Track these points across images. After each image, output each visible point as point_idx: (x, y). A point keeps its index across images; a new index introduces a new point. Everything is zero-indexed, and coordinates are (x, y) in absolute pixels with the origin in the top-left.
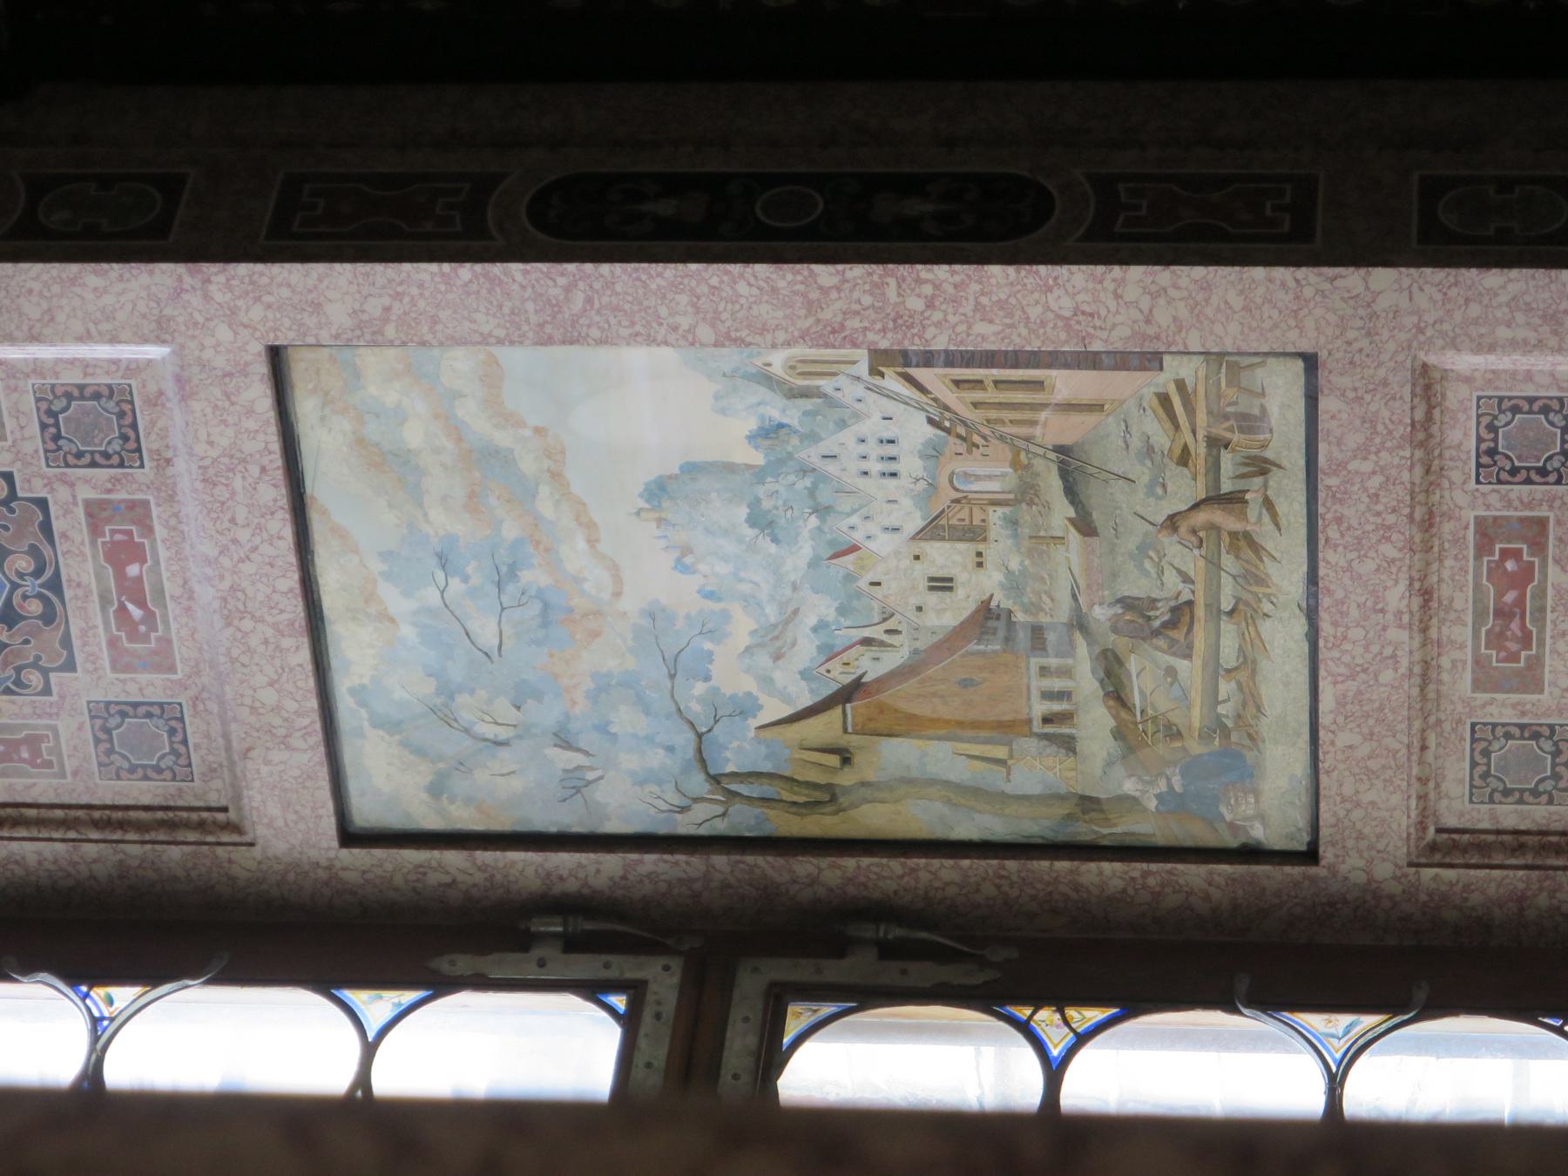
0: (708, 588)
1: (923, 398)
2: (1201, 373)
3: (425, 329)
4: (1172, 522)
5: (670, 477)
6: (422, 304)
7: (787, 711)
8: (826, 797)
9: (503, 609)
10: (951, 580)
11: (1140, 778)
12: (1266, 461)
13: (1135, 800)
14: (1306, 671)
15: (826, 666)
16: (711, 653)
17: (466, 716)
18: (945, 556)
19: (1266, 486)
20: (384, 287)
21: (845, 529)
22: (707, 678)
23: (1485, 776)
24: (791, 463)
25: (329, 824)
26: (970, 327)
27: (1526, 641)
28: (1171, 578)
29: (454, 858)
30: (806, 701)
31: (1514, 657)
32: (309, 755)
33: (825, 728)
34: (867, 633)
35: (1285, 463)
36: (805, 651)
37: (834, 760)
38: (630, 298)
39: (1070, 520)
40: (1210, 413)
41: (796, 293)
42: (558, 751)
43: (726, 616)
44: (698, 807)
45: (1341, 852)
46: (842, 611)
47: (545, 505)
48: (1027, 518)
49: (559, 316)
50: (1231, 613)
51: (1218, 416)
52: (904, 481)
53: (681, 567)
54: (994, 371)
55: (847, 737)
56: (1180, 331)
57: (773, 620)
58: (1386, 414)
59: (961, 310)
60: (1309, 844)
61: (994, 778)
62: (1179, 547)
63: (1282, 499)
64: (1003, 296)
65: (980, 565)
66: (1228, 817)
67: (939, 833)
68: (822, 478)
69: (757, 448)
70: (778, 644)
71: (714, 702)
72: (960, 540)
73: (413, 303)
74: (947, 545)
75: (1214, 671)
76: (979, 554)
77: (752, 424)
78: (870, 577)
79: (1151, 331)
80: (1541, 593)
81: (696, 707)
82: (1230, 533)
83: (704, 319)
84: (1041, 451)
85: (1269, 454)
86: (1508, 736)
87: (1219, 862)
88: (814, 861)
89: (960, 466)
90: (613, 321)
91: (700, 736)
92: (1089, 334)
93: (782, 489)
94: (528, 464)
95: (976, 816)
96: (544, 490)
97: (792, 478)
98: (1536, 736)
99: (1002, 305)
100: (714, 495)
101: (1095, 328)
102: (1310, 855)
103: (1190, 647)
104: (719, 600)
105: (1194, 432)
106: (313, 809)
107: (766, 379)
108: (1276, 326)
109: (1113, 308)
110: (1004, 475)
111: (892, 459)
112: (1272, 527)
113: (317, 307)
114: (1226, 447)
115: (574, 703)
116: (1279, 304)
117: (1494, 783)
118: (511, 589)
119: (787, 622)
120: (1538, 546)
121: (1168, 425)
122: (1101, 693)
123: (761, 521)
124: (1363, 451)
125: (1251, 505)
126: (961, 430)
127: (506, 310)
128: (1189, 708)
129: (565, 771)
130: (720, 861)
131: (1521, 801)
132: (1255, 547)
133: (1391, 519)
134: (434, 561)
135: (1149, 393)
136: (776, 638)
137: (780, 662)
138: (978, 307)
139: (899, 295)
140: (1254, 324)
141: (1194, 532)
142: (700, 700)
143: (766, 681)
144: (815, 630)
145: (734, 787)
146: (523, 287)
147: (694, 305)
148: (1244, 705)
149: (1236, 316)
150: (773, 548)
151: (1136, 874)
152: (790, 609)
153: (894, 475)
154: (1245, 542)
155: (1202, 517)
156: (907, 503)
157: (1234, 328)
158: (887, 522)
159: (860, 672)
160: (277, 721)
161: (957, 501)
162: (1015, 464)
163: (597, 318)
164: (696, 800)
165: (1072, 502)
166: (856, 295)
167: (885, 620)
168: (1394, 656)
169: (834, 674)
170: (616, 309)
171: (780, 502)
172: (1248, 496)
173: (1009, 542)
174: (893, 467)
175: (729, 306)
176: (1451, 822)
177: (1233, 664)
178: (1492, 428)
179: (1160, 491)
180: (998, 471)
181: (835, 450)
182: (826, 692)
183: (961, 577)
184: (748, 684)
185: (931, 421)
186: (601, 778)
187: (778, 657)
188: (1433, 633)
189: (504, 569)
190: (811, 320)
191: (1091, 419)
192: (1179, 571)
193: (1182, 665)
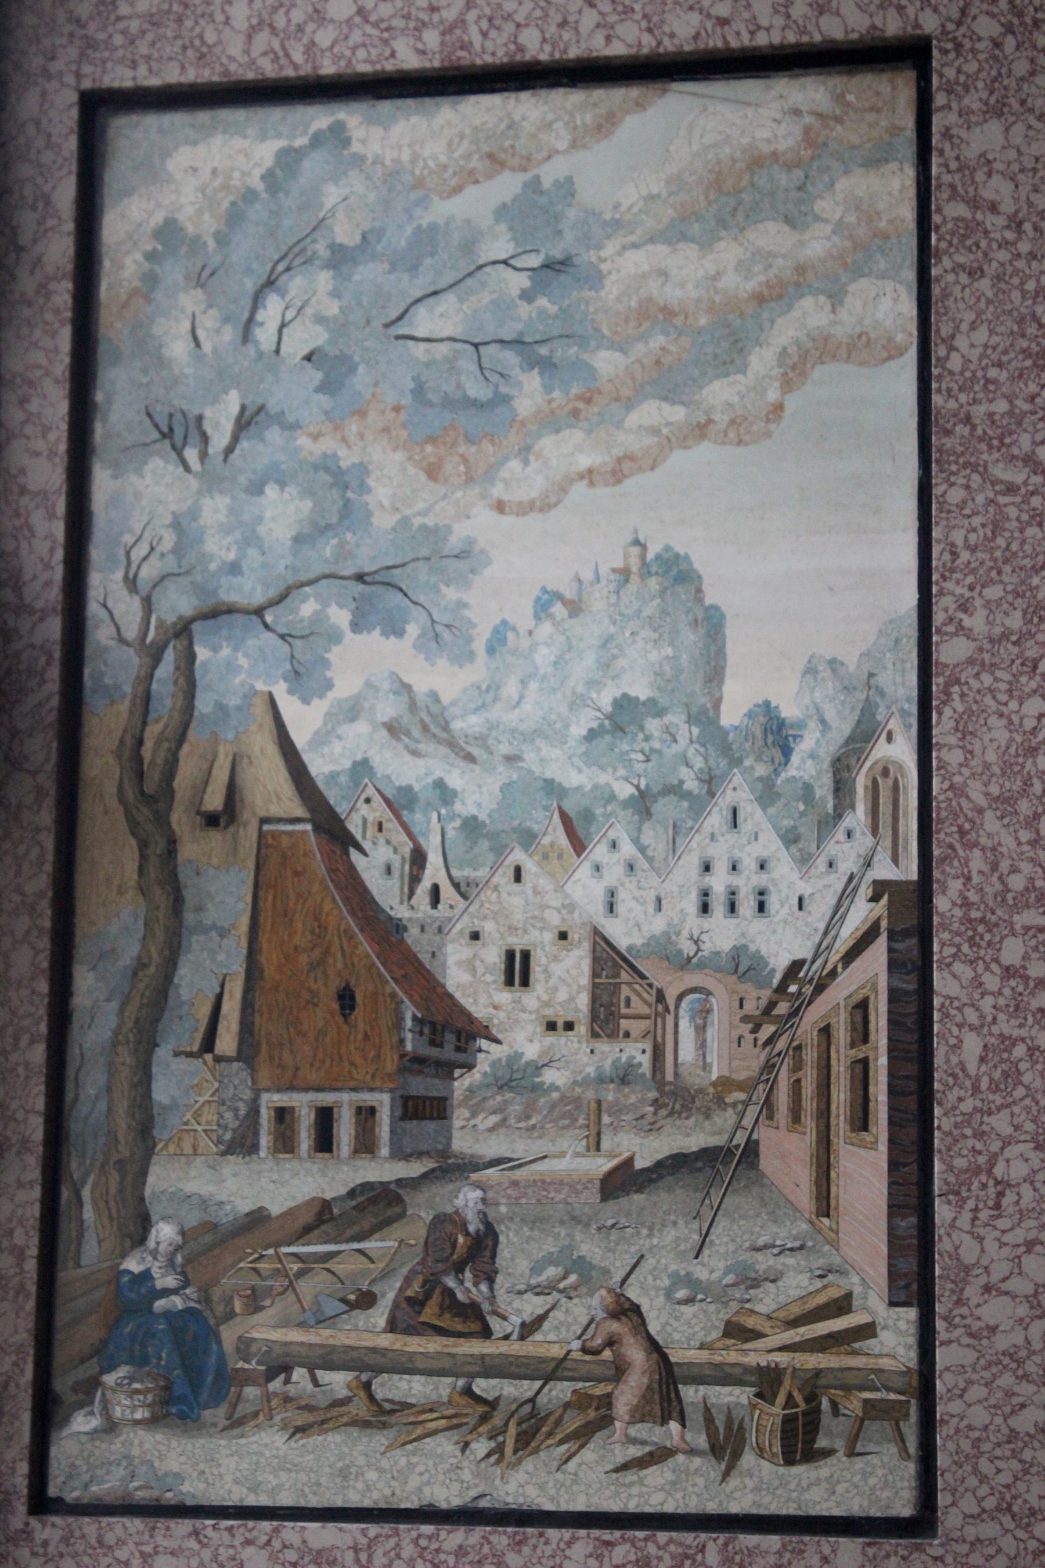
0: (510, 635)
1: (835, 957)
2: (886, 1363)
3: (960, 259)
4: (627, 1311)
5: (699, 590)
6: (1003, 255)
7: (300, 738)
8: (150, 787)
9: (476, 346)
10: (525, 982)
11: (178, 1248)
12: (736, 1455)
13: (142, 1240)
14: (367, 1503)
15: (377, 798)
16: (400, 633)
17: (296, 284)
18: (565, 979)
19: (692, 1452)
20: (1030, 204)
21: (612, 834)
22: (356, 627)
24: (723, 763)
26: (972, 1028)
28: (532, 1306)
29: (59, 249)
30: (317, 766)
32: (241, 56)
33: (270, 791)
34: (434, 859)
35: (733, 1482)
36: (402, 769)
37: (214, 801)
38: (1014, 547)
39: (629, 1161)
40: (818, 1373)
41: (1027, 783)
42: (235, 410)
43: (464, 657)
44: (136, 604)
45: (51, 1549)
46: (472, 826)
47: (652, 412)
48: (633, 1099)
49: (984, 447)
50: (468, 1392)
51: (813, 1386)
52: (693, 922)
53: (544, 604)
54: (883, 1060)
55: (254, 824)
56: (971, 1335)
57: (457, 725)
59: (1002, 1017)
60: (59, 1500)
62: (584, 1320)
63: (669, 1476)
64: (1027, 1078)
65: (551, 1026)
66: (109, 1379)
67: (84, 948)
68: (699, 806)
69: (750, 715)
70: (416, 732)
72: (594, 999)
73: (1004, 244)
74: (585, 980)
75: (367, 1365)
76: (569, 1026)
77: (789, 711)
78: (530, 866)
79: (972, 1292)
81: (308, 608)
82: (609, 1395)
83: (981, 650)
84: (748, 1122)
85: (748, 1459)
87: (37, 1364)
88: (50, 766)
89: (721, 1004)
90: (976, 521)
91: (259, 612)
92: (964, 1201)
93: (676, 749)
94: (721, 393)
95: (114, 1005)
96: (677, 414)
97: (699, 763)
99: (1013, 1075)
100: (669, 651)
101: (976, 1210)
102: (41, 1504)
103: (410, 1330)
104: (491, 650)
105: (782, 1349)
106: (148, 58)
107: (865, 733)
108: (983, 1479)
109: (1007, 1238)
110: (706, 1067)
111: (732, 908)
112: (620, 1459)
113: (997, 110)
114: (758, 1395)
115: (315, 437)
116: (1021, 1486)
118: (511, 358)
119: (452, 744)
121: (796, 1310)
122: (328, 1196)
123: (625, 716)
125: (658, 1430)
126: (782, 1008)
127: (993, 373)
128: (302, 1325)
129: (200, 419)
130: (54, 628)
132: (583, 1435)
134: (557, 254)
135: (853, 1282)
136: (425, 728)
137: (384, 733)
138: (1008, 1042)
139: (1027, 929)
140: (986, 1447)
141: (611, 1342)
142: (319, 617)
143: (352, 711)
144: (440, 784)
145: (169, 656)
146: (1032, 399)
147: (1005, 636)
148: (309, 1408)
149: (999, 1420)
150: (578, 730)
151: (19, 1238)
152: (475, 752)
153: (705, 908)
154: (597, 1417)
155: (636, 1354)
156: (657, 925)
157: (979, 1416)
158: (622, 895)
159: (367, 845)
160: (297, 16)
161: (661, 997)
162: (725, 1084)
163: (980, 499)
164: (148, 603)
165: (659, 1164)
166: (1026, 867)
167: (456, 886)
169: (364, 810)
170: (997, 527)
171: (656, 745)
172: (674, 1426)
173: (590, 1070)
174: (719, 908)
175: (1004, 687)
177: (379, 1394)
179: (681, 1294)
180: (712, 1058)
181: (746, 827)
182: (332, 796)
183: (530, 999)
184: (346, 685)
185: (797, 965)
186: (187, 468)
187: (393, 729)
189: (543, 350)
190: (982, 801)
191: (804, 1197)
192: (541, 1319)
193: (379, 1316)
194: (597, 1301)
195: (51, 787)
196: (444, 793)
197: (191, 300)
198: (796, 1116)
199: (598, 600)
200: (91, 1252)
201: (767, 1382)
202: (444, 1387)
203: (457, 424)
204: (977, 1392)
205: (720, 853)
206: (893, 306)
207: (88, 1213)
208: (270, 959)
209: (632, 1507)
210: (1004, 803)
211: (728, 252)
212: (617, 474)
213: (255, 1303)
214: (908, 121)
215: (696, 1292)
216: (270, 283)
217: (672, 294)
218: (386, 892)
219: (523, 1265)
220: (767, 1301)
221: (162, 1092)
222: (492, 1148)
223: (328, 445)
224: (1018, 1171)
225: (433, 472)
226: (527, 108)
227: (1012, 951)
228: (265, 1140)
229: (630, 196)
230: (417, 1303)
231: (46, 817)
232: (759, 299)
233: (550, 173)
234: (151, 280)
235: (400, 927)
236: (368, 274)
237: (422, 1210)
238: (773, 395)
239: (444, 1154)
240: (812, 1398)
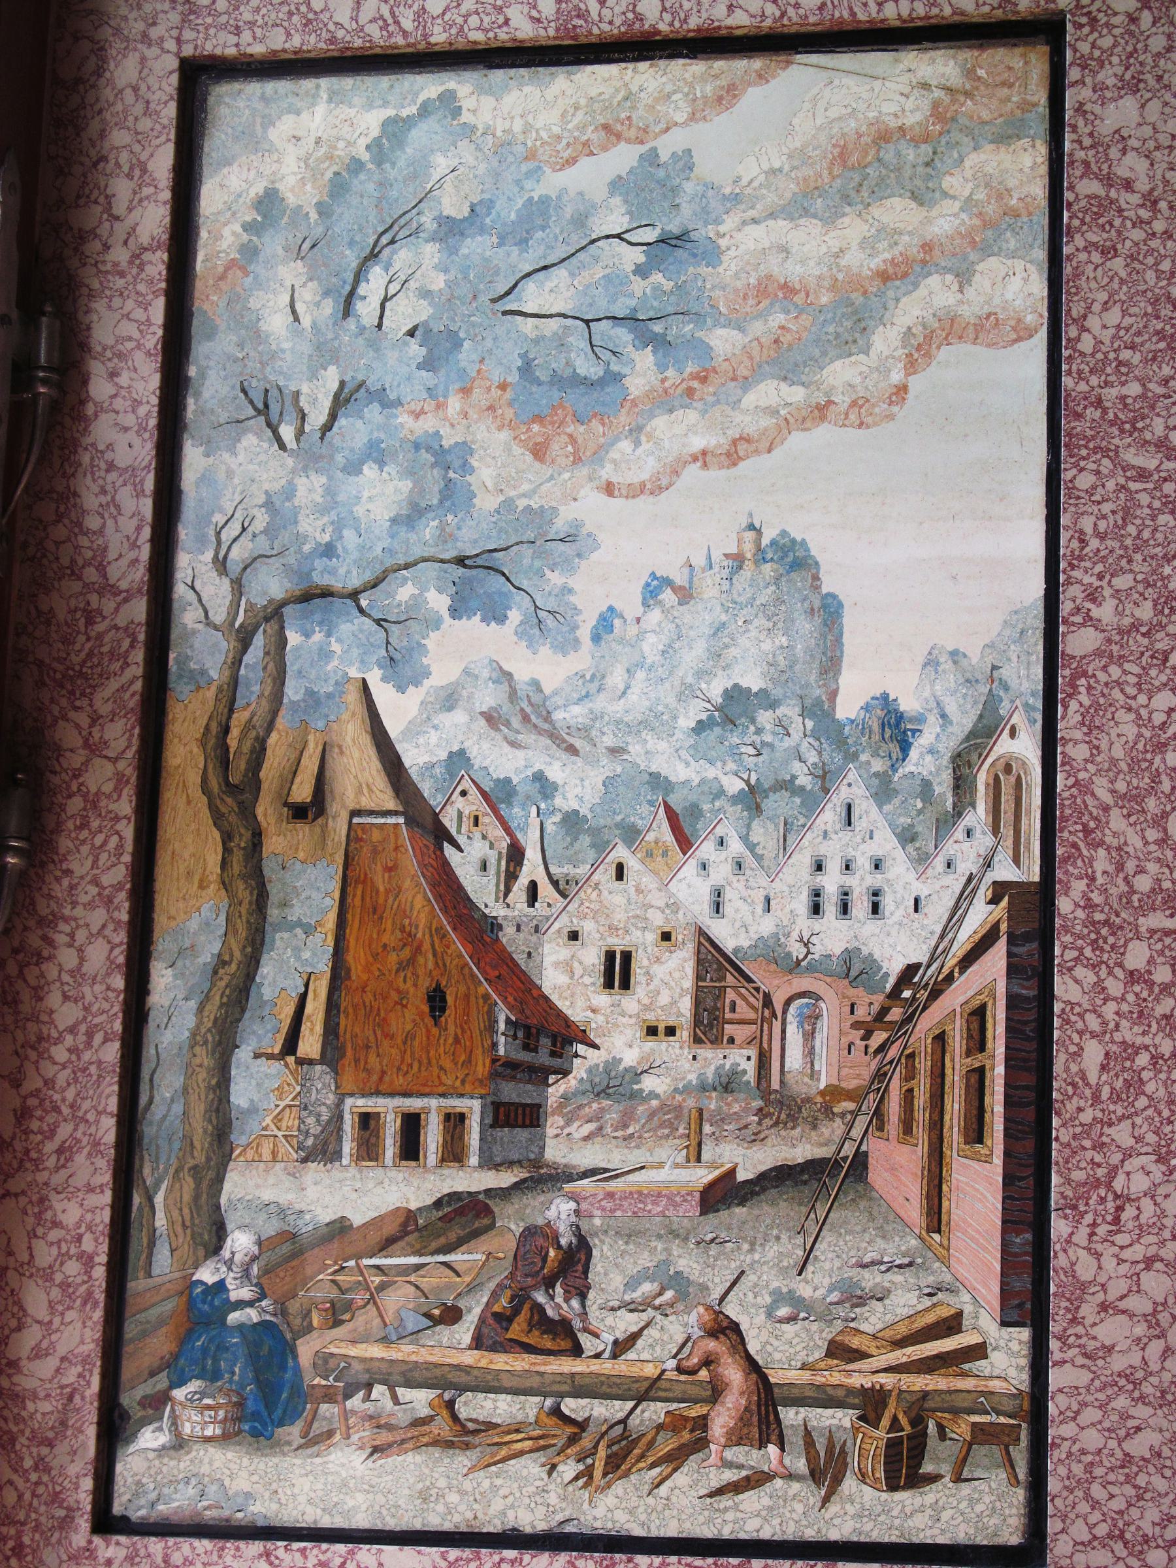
0: (617, 622)
1: (951, 962)
2: (996, 1385)
3: (1095, 238)
4: (725, 1329)
5: (816, 578)
6: (1137, 234)
8: (235, 778)
9: (587, 322)
10: (626, 985)
11: (254, 1258)
12: (837, 1480)
13: (217, 1249)
14: (447, 1526)
15: (473, 791)
16: (501, 620)
17: (402, 257)
18: (668, 982)
19: (790, 1476)
20: (1166, 182)
21: (719, 831)
22: (455, 612)
24: (838, 758)
25: (223, 45)
26: (1093, 1035)
28: (626, 1323)
29: (153, 219)
30: (413, 757)
33: (359, 781)
34: (532, 855)
35: (833, 1508)
36: (500, 760)
37: (302, 792)
38: (1146, 534)
39: (732, 1172)
40: (925, 1395)
41: (1156, 779)
42: (335, 386)
43: (570, 644)
44: (225, 585)
46: (572, 821)
47: (769, 393)
48: (736, 1108)
49: (1115, 431)
50: (556, 1412)
51: (920, 1408)
52: (804, 925)
54: (1000, 1070)
55: (344, 816)
56: (1085, 1355)
57: (558, 716)
59: (1124, 1023)
60: (125, 1519)
61: (260, 1034)
62: (680, 1339)
63: (766, 1501)
64: (1150, 1088)
65: (652, 1031)
66: (179, 1394)
67: (163, 944)
68: (812, 803)
69: (867, 708)
70: (516, 722)
71: (414, 617)
72: (697, 1003)
73: (1139, 223)
74: (688, 983)
75: (450, 1383)
76: (671, 1031)
77: (908, 704)
78: (633, 864)
79: (1087, 1311)
81: (405, 593)
82: (705, 1417)
83: (1109, 641)
84: (856, 1133)
85: (850, 1484)
87: (104, 1376)
88: (130, 754)
89: (831, 1009)
90: (1107, 508)
91: (354, 595)
92: (1082, 1215)
93: (788, 742)
94: (842, 375)
95: (193, 1004)
96: (796, 394)
97: (812, 758)
99: (1135, 1084)
100: (784, 641)
101: (1094, 1225)
102: (106, 1522)
103: (495, 1348)
104: (596, 638)
105: (886, 1370)
106: (252, 24)
107: (986, 730)
108: (1095, 1505)
109: (1126, 1254)
110: (814, 1075)
111: (845, 909)
112: (715, 1484)
113: (1133, 86)
114: (859, 1418)
115: (417, 415)
116: (1135, 1513)
118: (623, 336)
119: (553, 735)
121: (903, 1330)
122: (413, 1206)
123: (735, 709)
125: (755, 1454)
126: (896, 1014)
127: (1126, 355)
128: (385, 1340)
129: (297, 394)
130: (139, 610)
132: (676, 1459)
134: (674, 228)
135: (963, 1301)
136: (526, 718)
137: (483, 722)
138: (1131, 1050)
139: (1152, 932)
140: (1099, 1471)
141: (708, 1362)
142: (417, 602)
143: (449, 700)
144: (539, 777)
145: (259, 641)
146: (1165, 382)
147: (1135, 627)
148: (390, 1427)
149: (1113, 1444)
150: (687, 722)
151: (88, 1244)
152: (578, 743)
153: (816, 909)
155: (733, 1374)
156: (766, 926)
157: (1092, 1439)
158: (728, 894)
159: (461, 840)
161: (767, 1001)
162: (834, 1093)
163: (1111, 485)
164: (238, 587)
165: (762, 1176)
166: (1152, 867)
167: (555, 883)
169: (459, 802)
170: (1127, 514)
171: (768, 738)
172: (772, 1449)
173: (692, 1077)
174: (830, 908)
175: (1133, 680)
177: (463, 1412)
179: (783, 1312)
180: (820, 1065)
181: (860, 824)
182: (426, 788)
183: (630, 1003)
185: (911, 970)
186: (282, 446)
187: (492, 719)
189: (657, 328)
190: (1108, 799)
191: (914, 1212)
192: (634, 1337)
193: (464, 1332)
194: (693, 1320)
195: (132, 774)
196: (544, 785)
197: (291, 273)
198: (907, 1126)
199: (710, 587)
200: (163, 1260)
201: (870, 1404)
202: (530, 1408)
203: (564, 402)
204: (1091, 1415)
205: (833, 851)
206: (1020, 285)
207: (160, 1221)
208: (356, 958)
209: (726, 1533)
210: (1132, 801)
211: (853, 228)
212: (732, 457)
213: (336, 1315)
214: (1041, 97)
215: (799, 1310)
216: (374, 255)
217: (793, 271)
218: (481, 889)
219: (617, 1281)
220: (873, 1319)
221: (241, 1094)
222: (586, 1157)
223: (428, 424)
224: (1139, 1184)
225: (539, 452)
226: (646, 78)
227: (1137, 956)
228: (348, 1147)
229: (750, 170)
230: (504, 1319)
231: (125, 806)
232: (884, 277)
233: (667, 146)
234: (250, 252)
235: (495, 926)
236: (475, 246)
237: (511, 1221)
238: (896, 377)
239: (537, 1163)
240: (918, 1422)
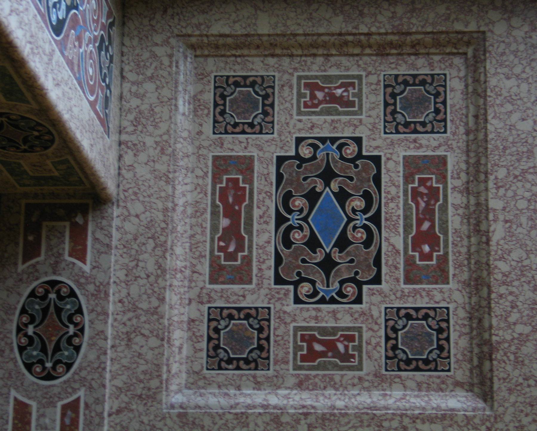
23: (437, 95)
27: (416, 193)
31: (422, 181)
45: (529, 40)
58: (509, 368)
80: (407, 227)
86: (423, 124)
98: (407, 124)
117: (431, 89)
120: (409, 262)
124: (523, 339)
131: (414, 76)
133: (503, 290)
168: (498, 188)
176: (458, 61)
178: (441, 348)
188: (473, 201)
